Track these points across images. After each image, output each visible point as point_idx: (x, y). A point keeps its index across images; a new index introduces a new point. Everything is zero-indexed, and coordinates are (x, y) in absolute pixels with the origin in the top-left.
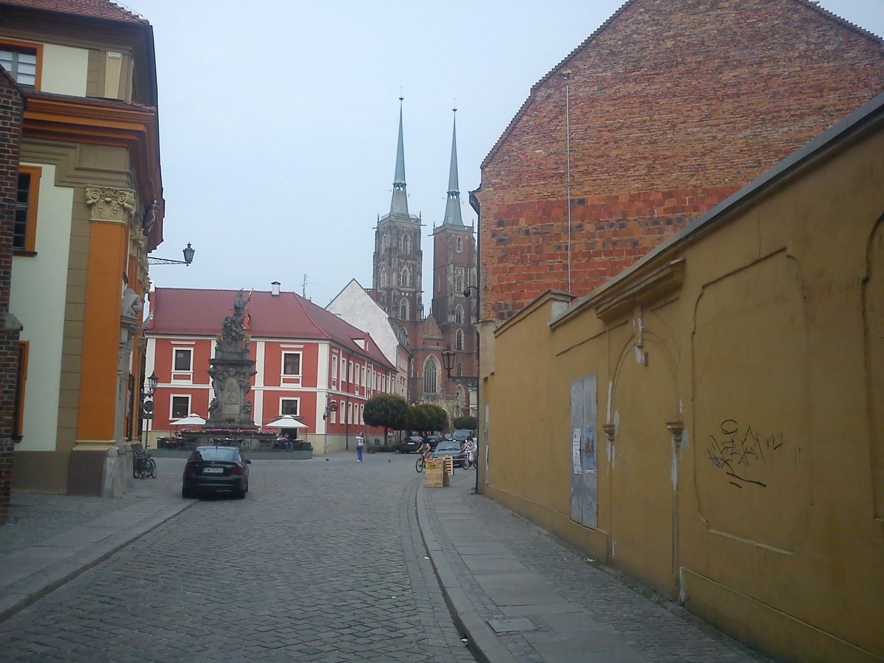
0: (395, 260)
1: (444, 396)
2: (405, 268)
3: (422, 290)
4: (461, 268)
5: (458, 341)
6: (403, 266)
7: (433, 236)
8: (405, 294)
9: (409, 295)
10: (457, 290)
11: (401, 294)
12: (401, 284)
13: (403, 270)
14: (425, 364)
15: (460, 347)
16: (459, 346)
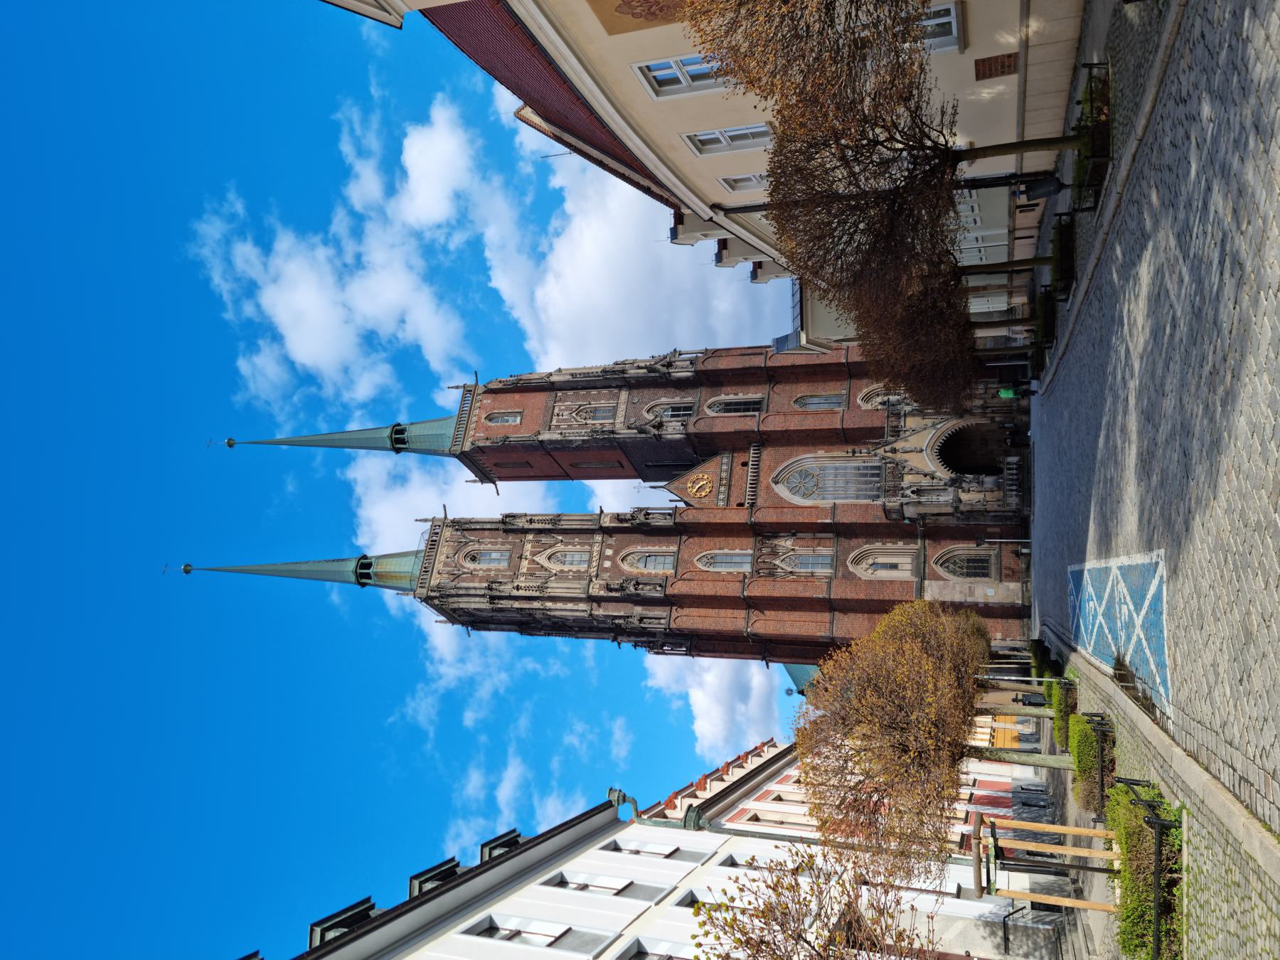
0: (518, 588)
1: (887, 444)
2: (542, 559)
3: (598, 512)
4: (556, 411)
5: (736, 411)
6: (538, 564)
7: (499, 483)
8: (608, 558)
9: (609, 547)
10: (608, 418)
11: (606, 570)
12: (583, 567)
13: (546, 564)
14: (797, 500)
15: (755, 403)
16: (751, 407)
